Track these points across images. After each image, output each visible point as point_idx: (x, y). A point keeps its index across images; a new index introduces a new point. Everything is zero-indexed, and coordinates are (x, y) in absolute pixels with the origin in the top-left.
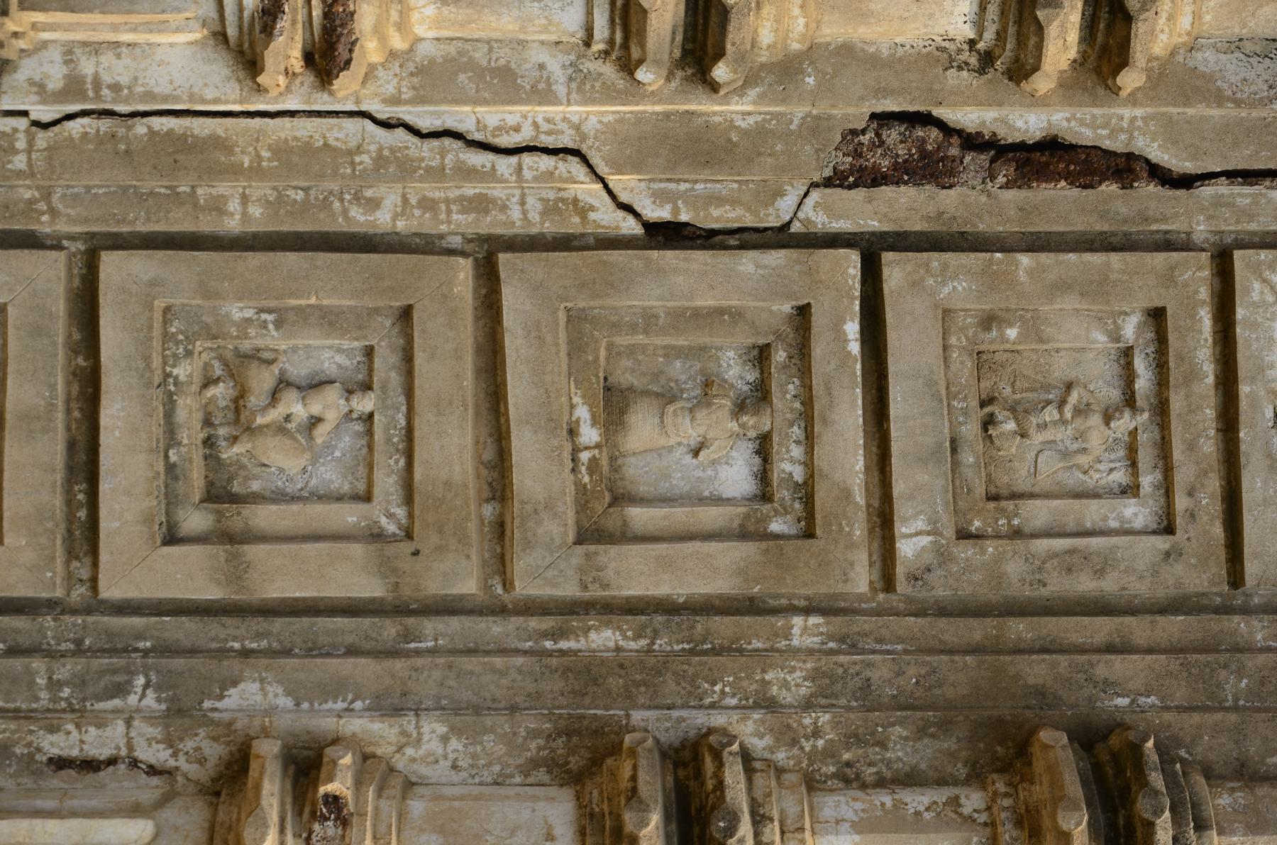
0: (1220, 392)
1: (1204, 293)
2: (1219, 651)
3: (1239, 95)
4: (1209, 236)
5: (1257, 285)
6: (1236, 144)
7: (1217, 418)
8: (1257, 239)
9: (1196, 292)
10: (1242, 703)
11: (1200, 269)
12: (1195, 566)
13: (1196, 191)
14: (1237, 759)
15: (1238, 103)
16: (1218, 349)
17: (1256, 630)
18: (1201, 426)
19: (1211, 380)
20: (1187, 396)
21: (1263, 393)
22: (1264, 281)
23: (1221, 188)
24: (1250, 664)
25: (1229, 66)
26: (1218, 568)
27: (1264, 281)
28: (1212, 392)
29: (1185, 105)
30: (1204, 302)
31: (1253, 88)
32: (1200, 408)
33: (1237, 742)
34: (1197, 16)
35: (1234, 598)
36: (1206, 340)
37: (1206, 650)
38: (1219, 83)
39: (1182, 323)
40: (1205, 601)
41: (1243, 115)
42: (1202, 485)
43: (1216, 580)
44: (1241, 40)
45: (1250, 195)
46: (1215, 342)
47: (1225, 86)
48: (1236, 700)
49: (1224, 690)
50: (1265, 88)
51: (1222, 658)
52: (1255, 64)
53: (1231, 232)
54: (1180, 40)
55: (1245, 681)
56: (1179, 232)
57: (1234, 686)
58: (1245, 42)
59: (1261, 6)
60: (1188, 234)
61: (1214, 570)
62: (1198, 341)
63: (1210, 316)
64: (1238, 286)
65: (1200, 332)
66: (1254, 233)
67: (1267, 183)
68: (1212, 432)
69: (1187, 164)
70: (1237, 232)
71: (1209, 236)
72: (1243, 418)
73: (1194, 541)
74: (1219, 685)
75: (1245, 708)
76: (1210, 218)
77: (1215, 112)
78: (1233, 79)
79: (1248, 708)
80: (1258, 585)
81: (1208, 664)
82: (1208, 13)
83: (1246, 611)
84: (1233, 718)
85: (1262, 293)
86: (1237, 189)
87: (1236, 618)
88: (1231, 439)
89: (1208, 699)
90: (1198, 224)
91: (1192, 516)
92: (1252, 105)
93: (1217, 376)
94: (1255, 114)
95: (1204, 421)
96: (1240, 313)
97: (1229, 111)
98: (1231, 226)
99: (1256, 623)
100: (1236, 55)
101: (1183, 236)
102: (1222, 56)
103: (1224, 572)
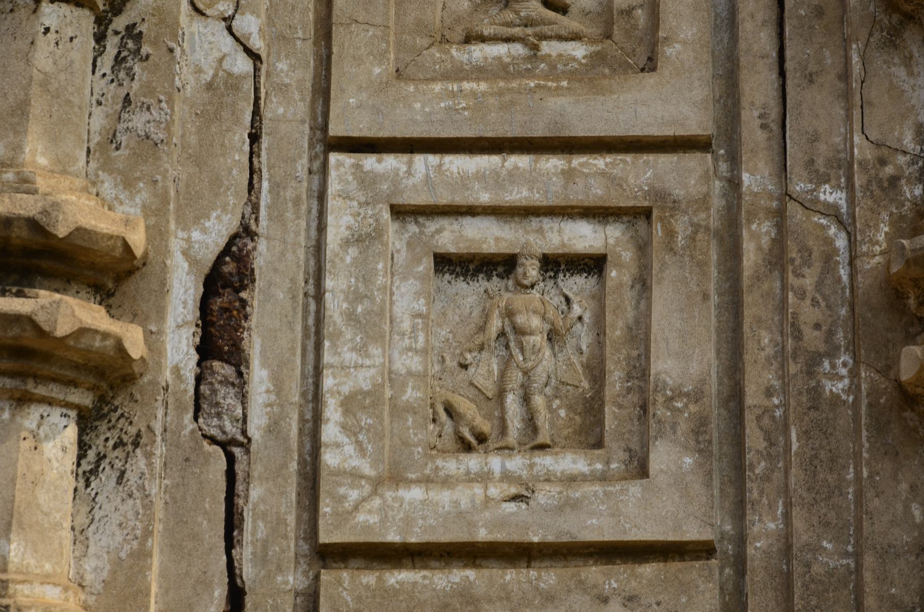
0: (484, 563)
1: (369, 578)
2: (789, 574)
3: (138, 533)
4: (300, 570)
5: (361, 517)
6: (195, 537)
7: (515, 567)
8: (305, 516)
9: (367, 587)
10: (850, 548)
11: (340, 582)
12: (690, 598)
13: (248, 584)
14: (918, 556)
15: (147, 533)
16: (433, 563)
17: (764, 529)
18: (525, 586)
19: (471, 573)
20: (490, 601)
21: (487, 514)
22: (356, 508)
23: (246, 554)
24: (805, 537)
25: (103, 543)
26: (692, 570)
27: (356, 508)
28: (486, 572)
29: (148, 595)
30: (380, 579)
31: (130, 515)
32: (504, 587)
33: (898, 556)
34: (46, 579)
35: (726, 553)
36: (424, 577)
37: (788, 587)
38: (123, 555)
39: (404, 605)
40: (730, 586)
41: (161, 527)
42: (595, 586)
43: (706, 573)
44: (73, 529)
45: (254, 521)
46: (425, 567)
47: (127, 548)
48: (847, 554)
49: (836, 568)
50: (131, 502)
51: (798, 569)
52: (102, 513)
53: (296, 545)
54: (71, 600)
55: (825, 544)
56: (295, 605)
57: (830, 556)
58: (76, 523)
59: (38, 506)
60: (297, 594)
61: (694, 575)
62: (425, 586)
63: (396, 573)
64: (362, 539)
65: (415, 584)
66: (299, 518)
67: (241, 502)
68: (533, 573)
69: (216, 594)
70: (297, 538)
71: (300, 570)
72: (516, 538)
73: (660, 598)
74: (830, 573)
75: (857, 544)
76: (279, 569)
77: (156, 561)
78: (119, 538)
79: (857, 542)
80: (712, 525)
81: (805, 586)
82: (42, 567)
83: (741, 540)
84: (869, 560)
85: (370, 512)
86: (247, 537)
87: (750, 551)
88: (540, 551)
89: (846, 586)
90: (286, 583)
91: (631, 599)
92: (150, 518)
93: (466, 566)
94: (159, 514)
95: (519, 582)
96: (393, 537)
97: (155, 544)
98: (290, 545)
99: (755, 529)
100: (90, 534)
101: (299, 600)
102: (92, 550)
103: (697, 564)
